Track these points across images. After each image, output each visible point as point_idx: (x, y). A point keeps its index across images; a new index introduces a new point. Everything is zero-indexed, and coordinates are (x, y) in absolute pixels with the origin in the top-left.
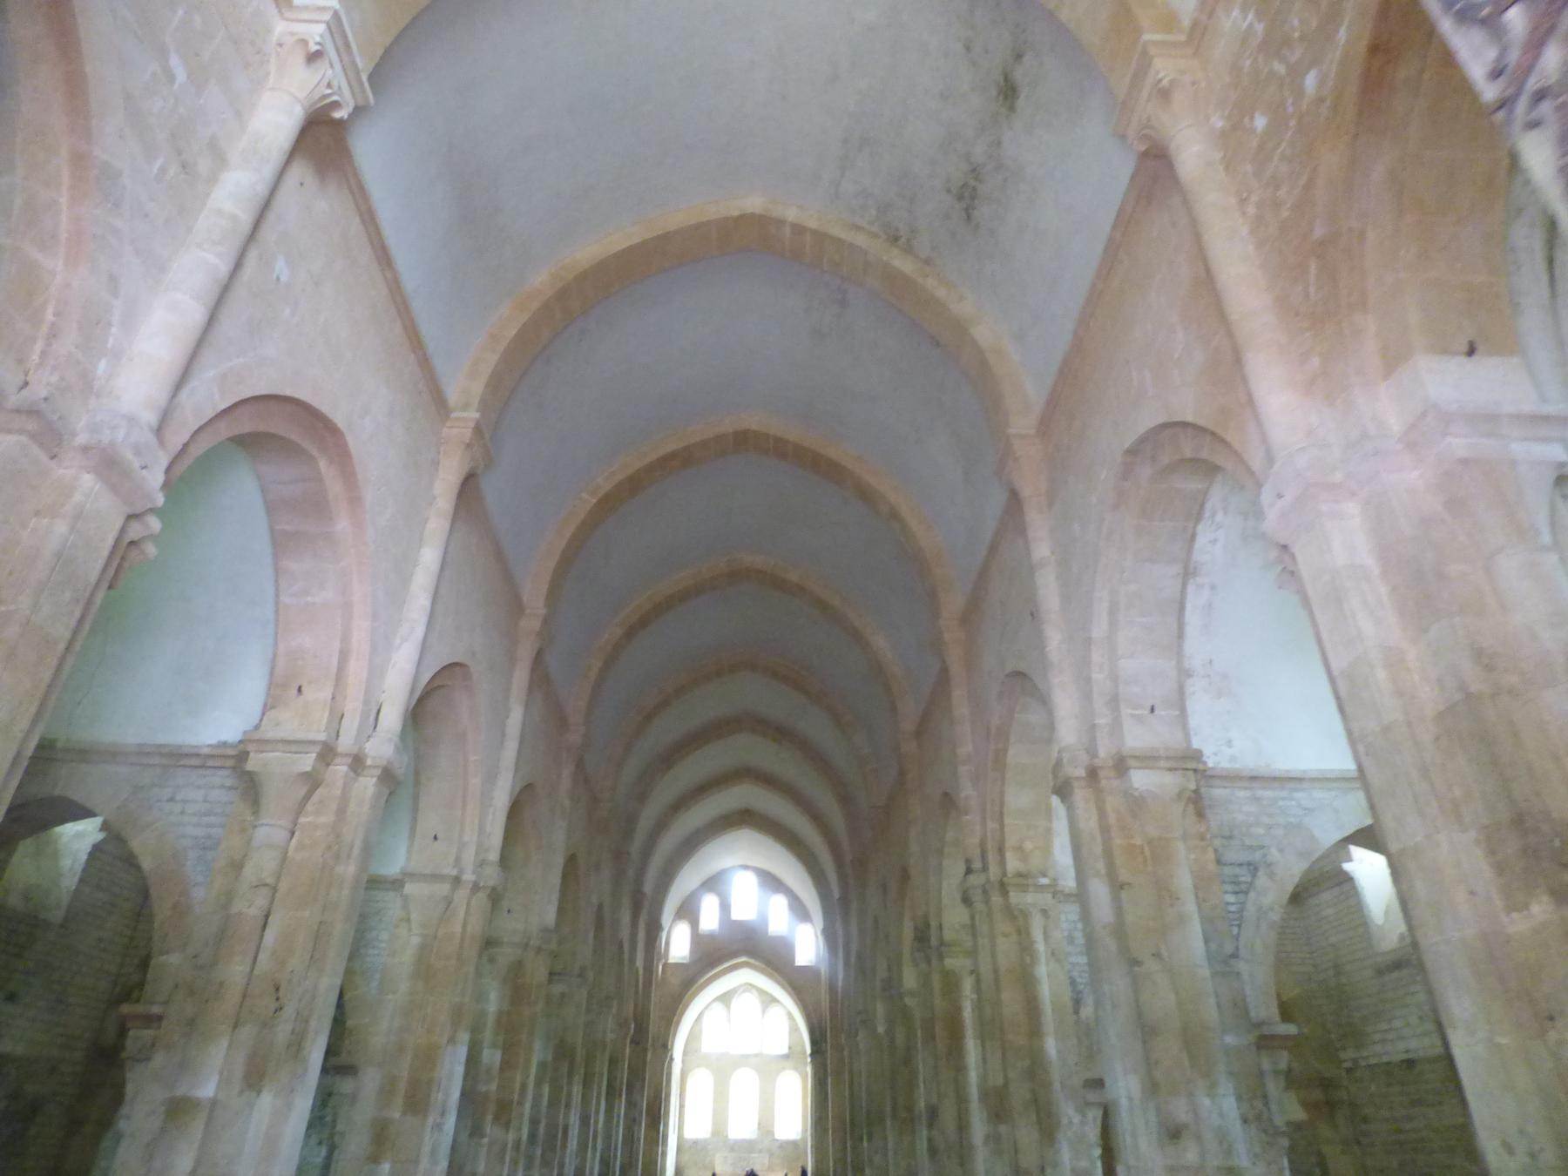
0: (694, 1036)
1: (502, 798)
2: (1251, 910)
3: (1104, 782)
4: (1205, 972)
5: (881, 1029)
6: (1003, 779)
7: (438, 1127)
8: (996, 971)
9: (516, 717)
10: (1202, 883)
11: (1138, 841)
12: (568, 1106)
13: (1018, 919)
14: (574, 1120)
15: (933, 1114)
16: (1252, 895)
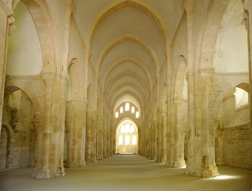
0: (120, 130)
5: (150, 127)
7: (83, 140)
12: (101, 139)
14: (102, 141)
15: (158, 139)
16: (218, 97)
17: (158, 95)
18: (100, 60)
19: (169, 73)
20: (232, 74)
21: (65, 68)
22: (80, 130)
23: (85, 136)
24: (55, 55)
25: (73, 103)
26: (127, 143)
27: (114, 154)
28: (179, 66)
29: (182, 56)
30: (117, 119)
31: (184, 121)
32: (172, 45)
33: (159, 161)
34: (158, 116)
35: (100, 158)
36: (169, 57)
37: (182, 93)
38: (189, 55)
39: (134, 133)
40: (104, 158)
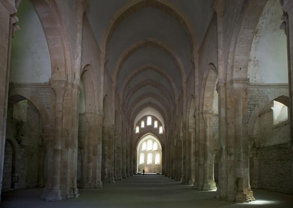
0: (141, 147)
1: (102, 97)
2: (253, 114)
3: (227, 86)
4: (241, 126)
5: (175, 144)
6: (204, 90)
7: (99, 158)
8: (199, 130)
9: (102, 79)
10: (244, 108)
11: (232, 100)
13: (205, 120)
15: (185, 157)
17: (184, 108)
18: (117, 67)
19: (197, 84)
20: (268, 86)
21: (78, 76)
22: (96, 146)
23: (101, 153)
24: (65, 61)
25: (87, 115)
26: (149, 162)
27: (135, 174)
28: (208, 74)
29: (211, 64)
30: (137, 134)
31: (215, 137)
32: (200, 51)
33: (186, 183)
34: (185, 131)
35: (119, 178)
36: (196, 64)
37: (212, 106)
38: (219, 63)
39: (157, 151)
40: (123, 178)
